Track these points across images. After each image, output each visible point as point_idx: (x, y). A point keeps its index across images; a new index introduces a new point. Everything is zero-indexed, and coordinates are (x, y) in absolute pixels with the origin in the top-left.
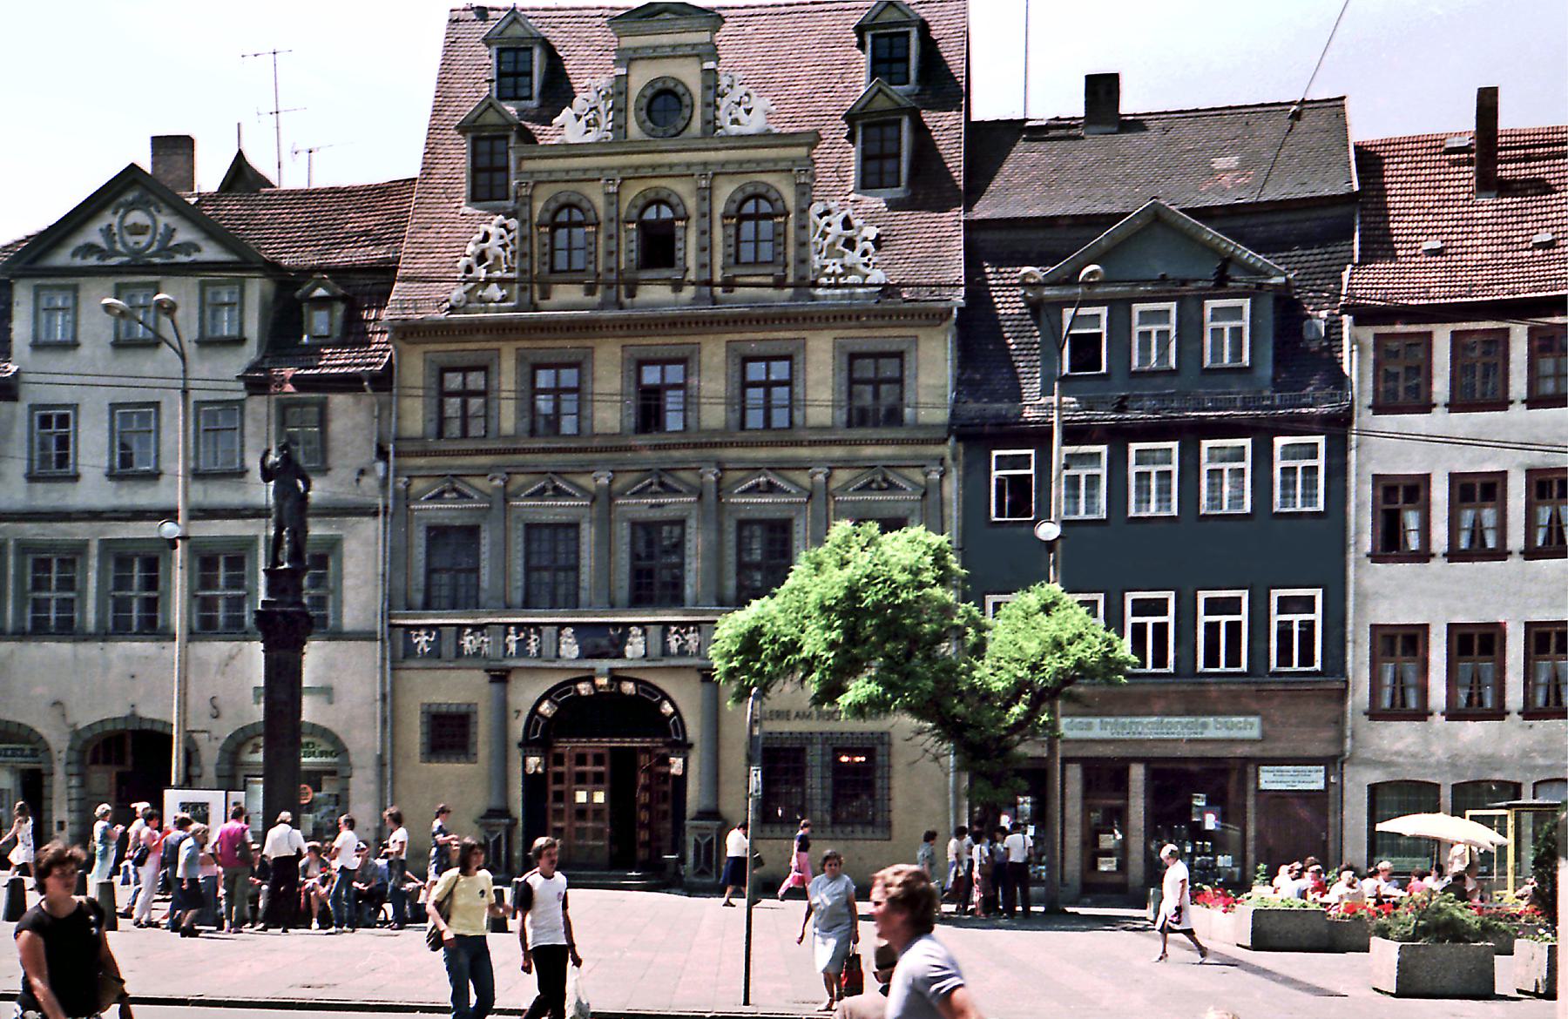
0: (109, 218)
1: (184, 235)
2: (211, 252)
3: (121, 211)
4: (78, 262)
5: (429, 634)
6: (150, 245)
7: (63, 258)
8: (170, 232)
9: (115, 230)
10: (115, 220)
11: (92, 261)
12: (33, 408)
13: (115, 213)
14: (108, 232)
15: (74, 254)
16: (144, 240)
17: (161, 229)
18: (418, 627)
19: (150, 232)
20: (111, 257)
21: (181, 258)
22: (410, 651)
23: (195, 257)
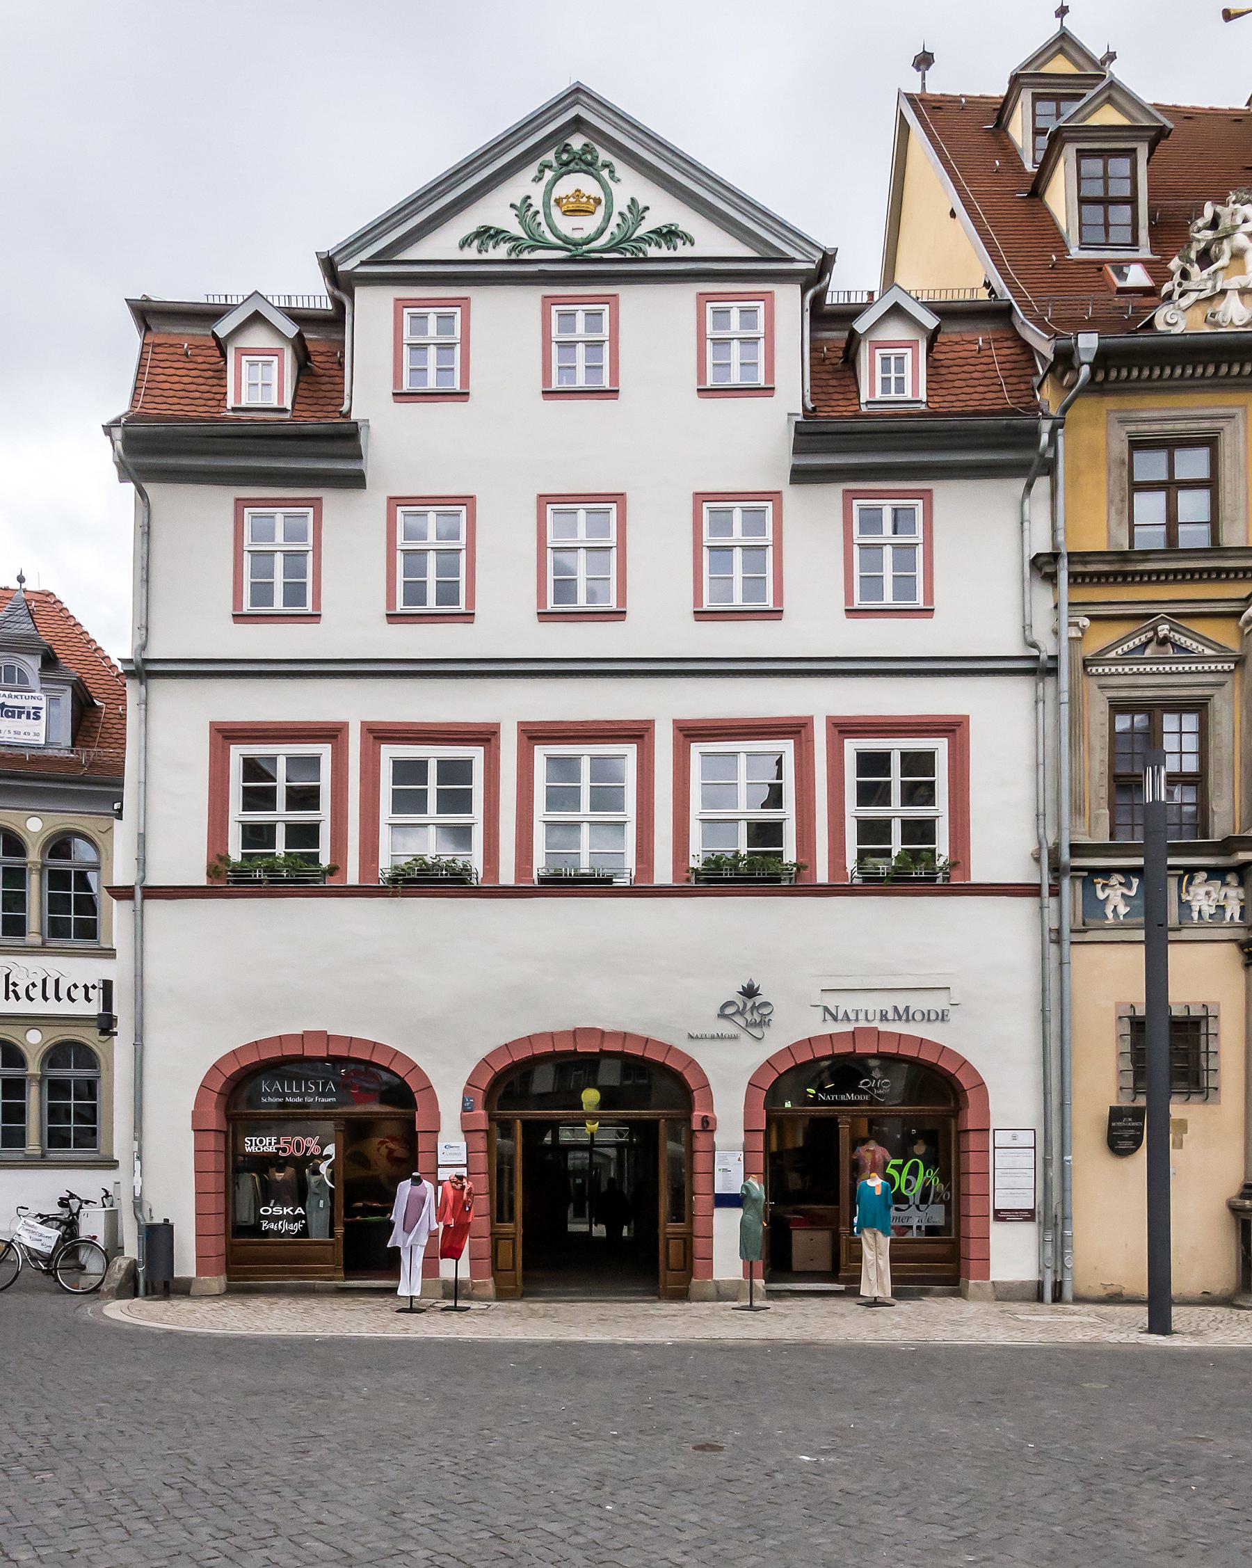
0: (524, 185)
1: (664, 210)
2: (710, 241)
3: (549, 174)
4: (471, 253)
5: (1128, 885)
6: (601, 232)
7: (443, 245)
8: (637, 211)
9: (537, 204)
10: (537, 193)
11: (501, 252)
12: (395, 502)
13: (538, 179)
14: (523, 208)
15: (465, 243)
16: (587, 225)
17: (621, 204)
18: (1107, 872)
19: (601, 211)
20: (533, 248)
21: (653, 252)
22: (1093, 907)
23: (683, 250)
